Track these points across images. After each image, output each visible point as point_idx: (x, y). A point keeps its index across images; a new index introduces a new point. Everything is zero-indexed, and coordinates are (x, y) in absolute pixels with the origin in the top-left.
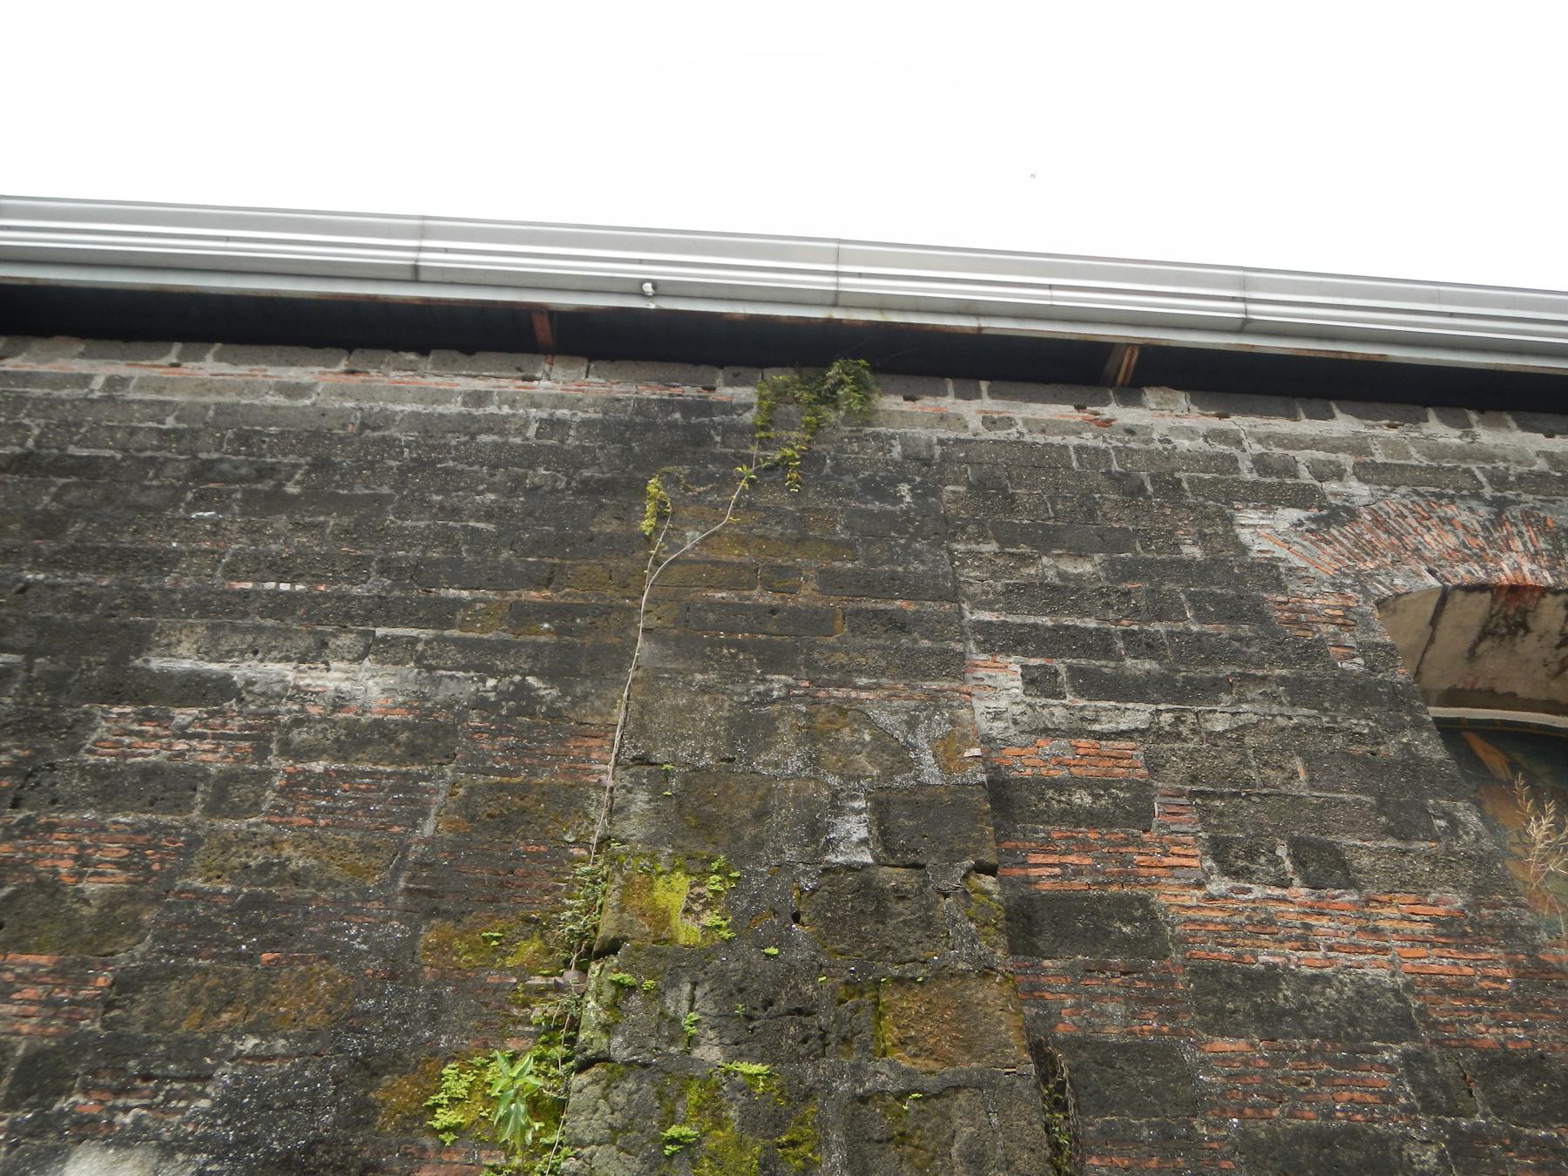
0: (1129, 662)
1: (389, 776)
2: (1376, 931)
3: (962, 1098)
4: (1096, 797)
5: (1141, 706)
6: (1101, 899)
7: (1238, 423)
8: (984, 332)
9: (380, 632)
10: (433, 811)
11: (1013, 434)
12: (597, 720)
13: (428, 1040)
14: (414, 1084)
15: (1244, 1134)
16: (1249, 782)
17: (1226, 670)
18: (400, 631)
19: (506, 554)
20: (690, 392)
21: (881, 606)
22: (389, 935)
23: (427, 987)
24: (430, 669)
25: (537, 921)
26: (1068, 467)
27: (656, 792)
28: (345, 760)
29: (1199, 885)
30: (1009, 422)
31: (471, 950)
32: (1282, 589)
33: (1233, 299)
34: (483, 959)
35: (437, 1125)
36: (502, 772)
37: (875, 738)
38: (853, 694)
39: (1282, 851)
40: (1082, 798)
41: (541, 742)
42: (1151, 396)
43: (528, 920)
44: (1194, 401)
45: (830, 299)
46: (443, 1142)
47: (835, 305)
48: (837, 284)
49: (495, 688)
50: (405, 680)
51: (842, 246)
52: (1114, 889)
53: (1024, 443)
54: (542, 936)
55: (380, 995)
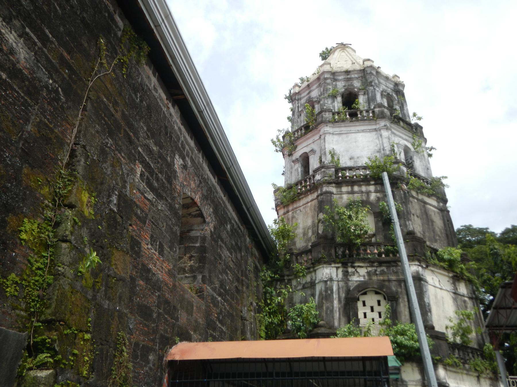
0: (154, 182)
1: (22, 97)
2: (162, 268)
3: (121, 282)
4: (141, 213)
5: (152, 194)
6: (135, 239)
7: (182, 128)
8: (171, 67)
9: (27, 30)
10: (31, 121)
11: (157, 95)
12: (71, 119)
13: (21, 207)
14: (16, 220)
15: (139, 302)
16: (158, 224)
17: (164, 195)
18: (32, 35)
19: (62, 29)
20: (111, 9)
21: (129, 132)
22: (15, 162)
23: (23, 188)
24: (38, 61)
25: (49, 182)
26: (161, 116)
27: (86, 161)
28: (11, 79)
29: (147, 244)
30: (156, 91)
31: (34, 182)
32: (175, 180)
33: (204, 105)
34: (36, 187)
35: (21, 237)
36: (48, 120)
37: (122, 174)
38: (121, 157)
39: (158, 243)
40: (139, 212)
41: (58, 116)
42: (176, 107)
43: (47, 180)
44: (180, 115)
45: (156, 24)
46: (21, 243)
47: (155, 26)
48: (161, 23)
49: (51, 85)
50: (30, 59)
51: (170, 16)
52: (137, 238)
53: (157, 100)
54: (49, 187)
55: (12, 184)
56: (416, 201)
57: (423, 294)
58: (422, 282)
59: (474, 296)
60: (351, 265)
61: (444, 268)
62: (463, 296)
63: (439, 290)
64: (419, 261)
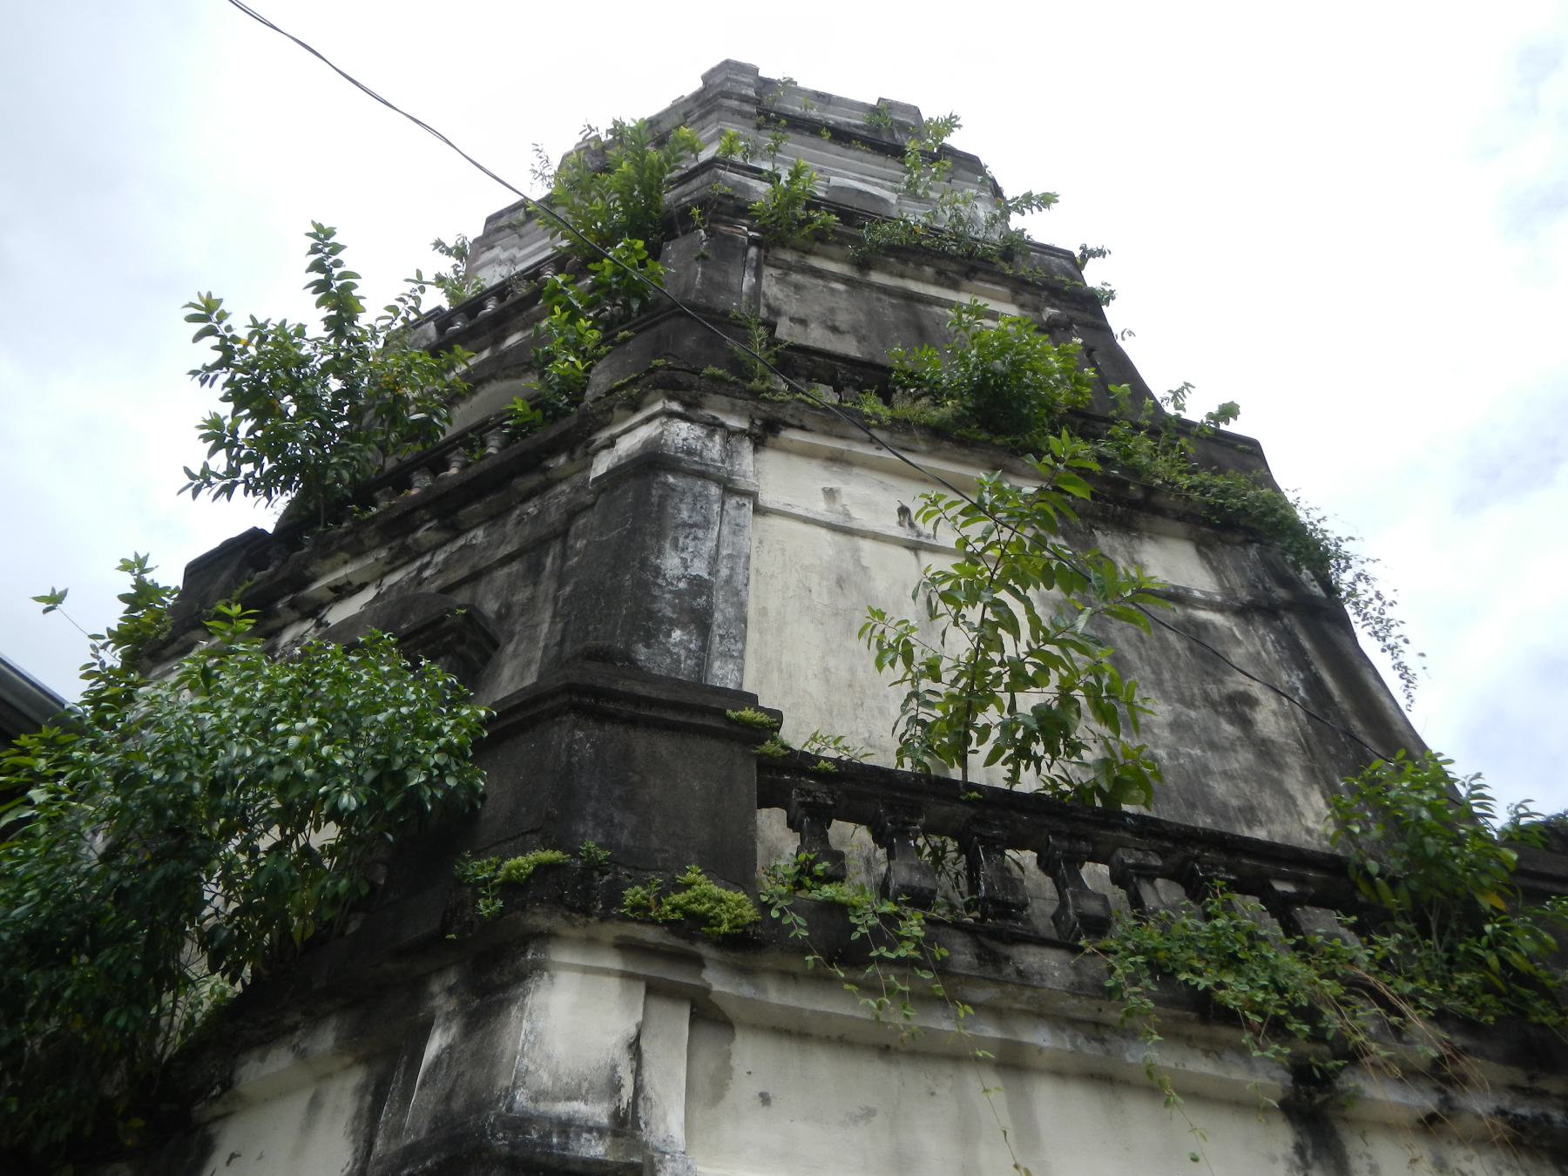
56: (840, 287)
57: (660, 535)
58: (671, 479)
59: (1281, 594)
60: (293, 606)
61: (939, 436)
62: (1178, 597)
63: (907, 555)
64: (671, 388)
